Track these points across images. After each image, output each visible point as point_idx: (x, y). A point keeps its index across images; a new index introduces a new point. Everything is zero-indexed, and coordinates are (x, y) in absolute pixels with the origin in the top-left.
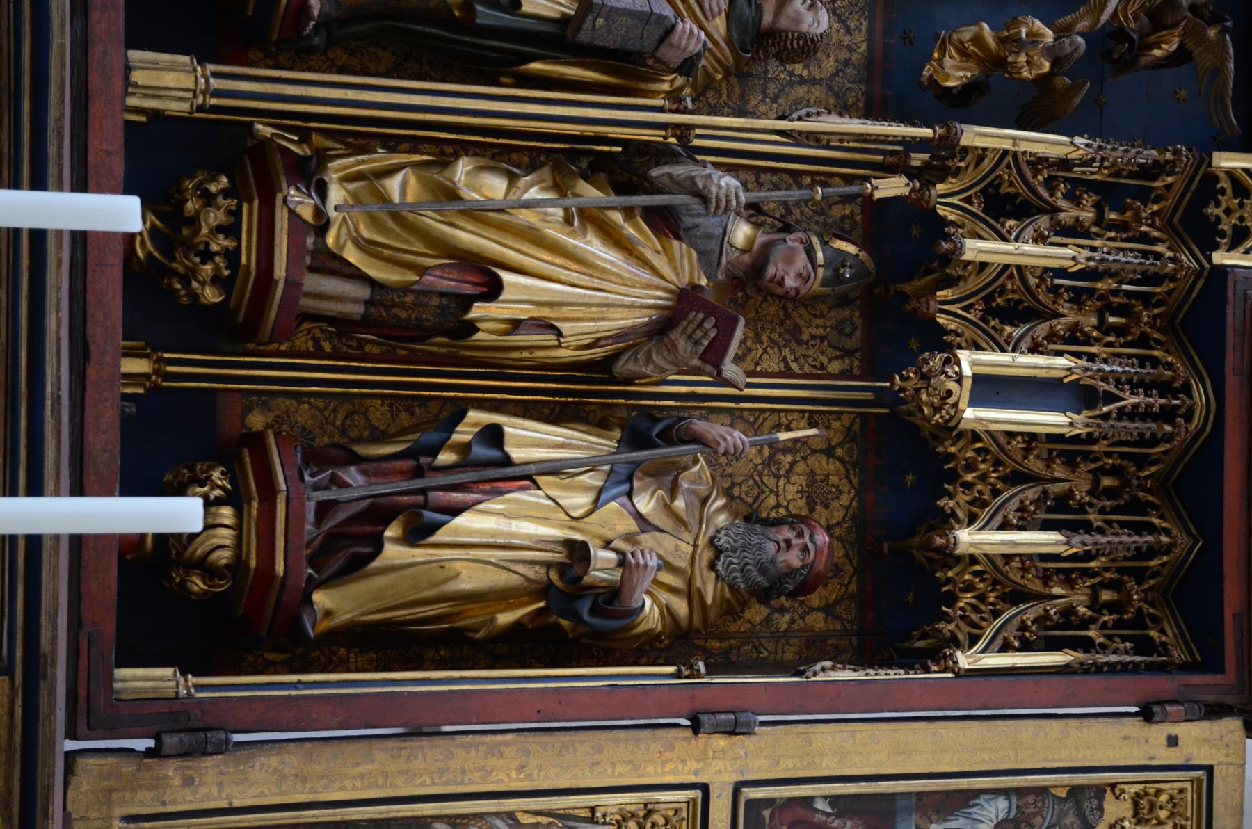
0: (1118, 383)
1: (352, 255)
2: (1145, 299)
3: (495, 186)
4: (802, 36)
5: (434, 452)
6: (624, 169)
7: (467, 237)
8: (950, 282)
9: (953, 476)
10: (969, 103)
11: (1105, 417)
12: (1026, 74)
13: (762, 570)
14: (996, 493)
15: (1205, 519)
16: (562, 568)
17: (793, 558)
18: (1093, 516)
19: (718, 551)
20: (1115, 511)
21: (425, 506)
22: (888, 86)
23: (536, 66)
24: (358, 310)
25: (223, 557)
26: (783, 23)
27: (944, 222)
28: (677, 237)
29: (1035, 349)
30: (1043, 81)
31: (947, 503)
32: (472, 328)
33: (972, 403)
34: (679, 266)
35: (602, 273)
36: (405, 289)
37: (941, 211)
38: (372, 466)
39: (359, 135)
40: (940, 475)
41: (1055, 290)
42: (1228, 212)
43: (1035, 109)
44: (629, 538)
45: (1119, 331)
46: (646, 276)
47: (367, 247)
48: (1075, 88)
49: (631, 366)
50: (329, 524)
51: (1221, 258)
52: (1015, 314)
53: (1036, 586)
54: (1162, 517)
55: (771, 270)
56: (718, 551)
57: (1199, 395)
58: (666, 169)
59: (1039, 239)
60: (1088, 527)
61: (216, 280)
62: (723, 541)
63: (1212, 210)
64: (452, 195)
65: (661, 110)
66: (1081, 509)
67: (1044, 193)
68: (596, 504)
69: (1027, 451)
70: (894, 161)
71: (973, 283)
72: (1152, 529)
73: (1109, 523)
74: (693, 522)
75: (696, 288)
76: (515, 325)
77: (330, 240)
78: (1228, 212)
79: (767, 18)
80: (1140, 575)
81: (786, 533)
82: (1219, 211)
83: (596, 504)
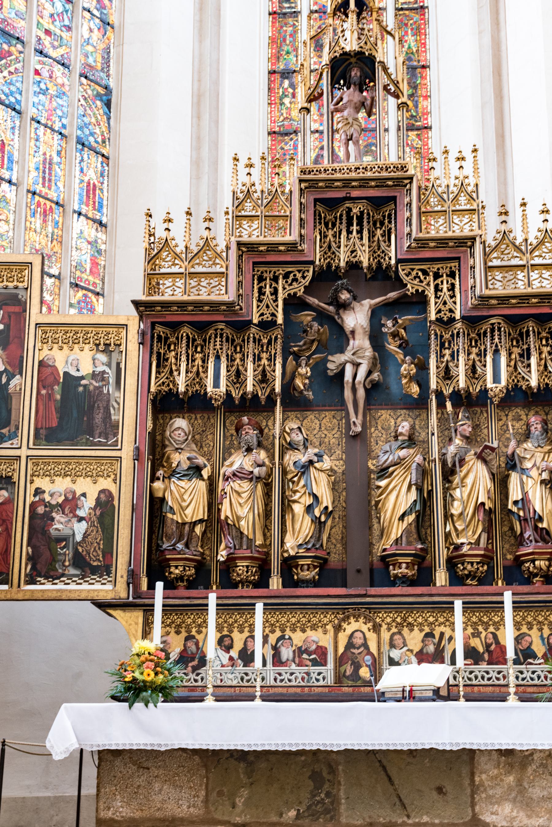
0: (492, 343)
1: (476, 537)
2: (468, 335)
3: (456, 504)
4: (410, 429)
5: (519, 516)
6: (449, 473)
7: (470, 510)
8: (468, 387)
9: (516, 385)
10: (423, 384)
11: (501, 346)
12: (415, 371)
13: (542, 435)
14: (520, 373)
15: (524, 318)
16: (546, 485)
17: (539, 426)
18: (525, 347)
19: (539, 446)
20: (523, 341)
21: (534, 518)
22: (419, 404)
23: (425, 495)
24: (486, 534)
25: (547, 563)
26: (407, 434)
27: (454, 391)
28: (464, 459)
29: (485, 366)
30: (416, 365)
31: (524, 387)
32: (490, 508)
33: (500, 383)
34: (470, 457)
35: (476, 477)
36: (484, 525)
37: (450, 392)
38: (524, 531)
39: (448, 535)
40: (516, 388)
41: (468, 360)
42: (445, 314)
43: (423, 367)
44: (538, 469)
45: (476, 341)
46: (475, 467)
47: (474, 533)
48: (419, 358)
49: (495, 469)
50: (539, 539)
51: (458, 316)
52: (473, 369)
53: (543, 362)
54: (524, 328)
55: (468, 435)
56: (539, 446)
57: (493, 321)
58: (449, 463)
59: (457, 366)
60: (528, 349)
61: (482, 567)
62: (536, 445)
63: (445, 319)
64: (461, 514)
65: (435, 465)
66: (523, 350)
67: (444, 364)
68: (531, 477)
69: (510, 366)
70: (441, 405)
71: (469, 383)
72: (528, 332)
73: (526, 343)
74: (532, 453)
75: (475, 454)
76: (489, 498)
77: (473, 541)
78: (445, 314)
79: (406, 438)
80: (539, 333)
81: (533, 428)
82: (445, 317)
83: (531, 477)
